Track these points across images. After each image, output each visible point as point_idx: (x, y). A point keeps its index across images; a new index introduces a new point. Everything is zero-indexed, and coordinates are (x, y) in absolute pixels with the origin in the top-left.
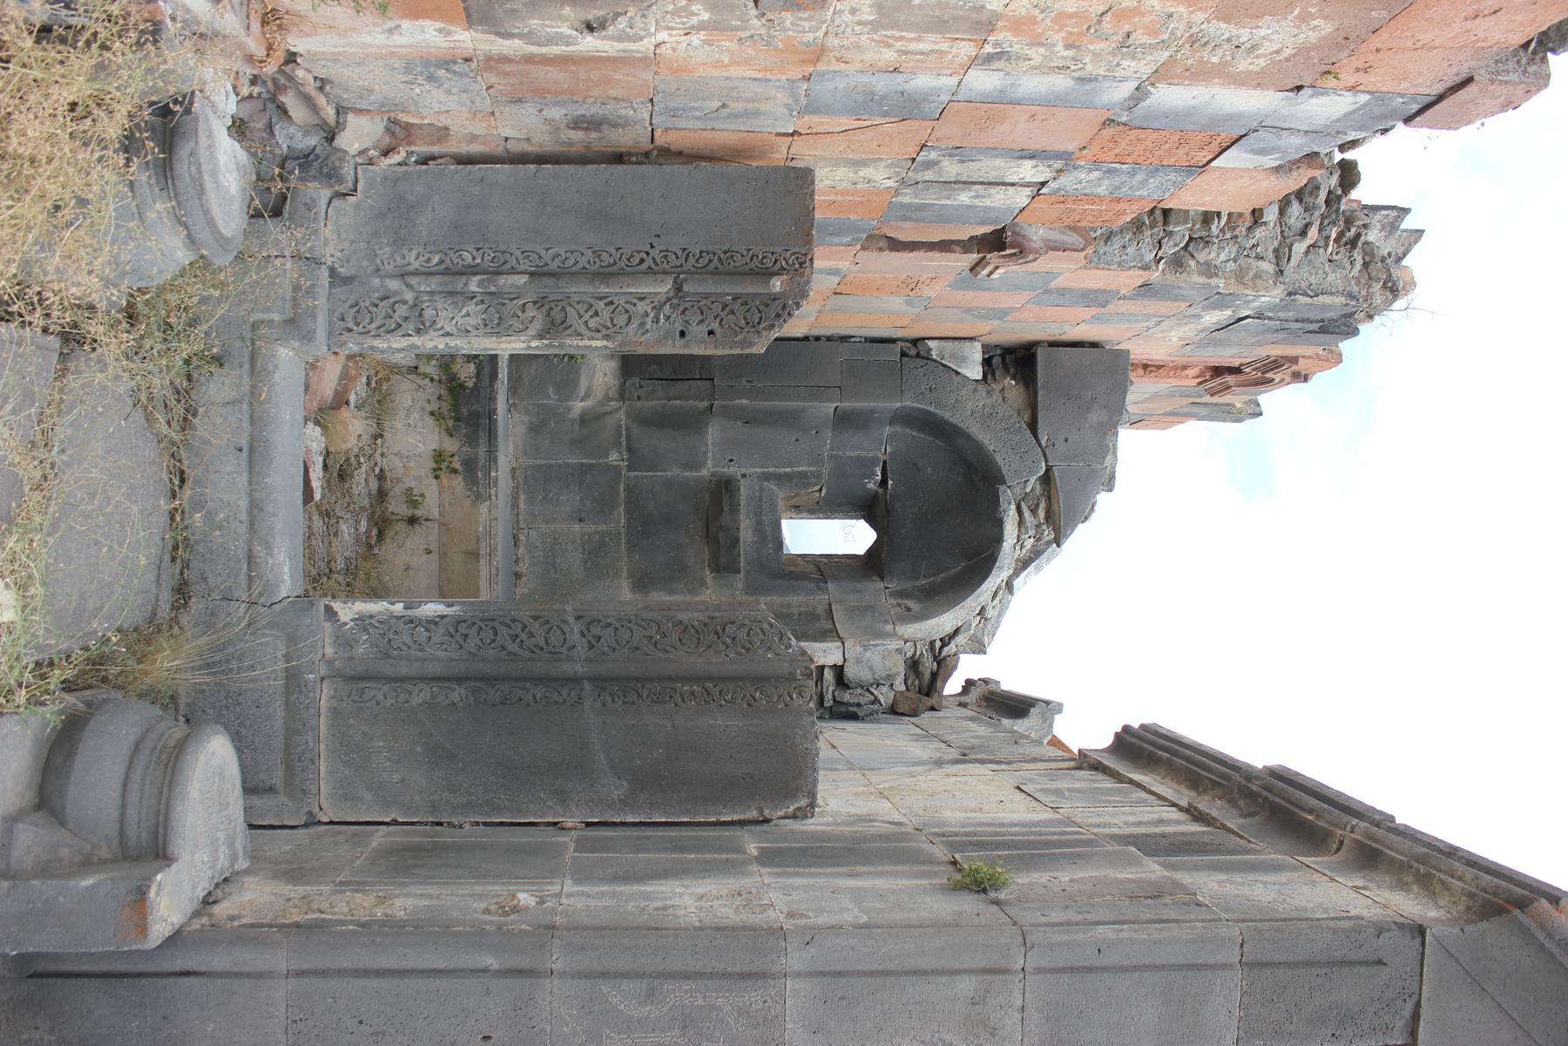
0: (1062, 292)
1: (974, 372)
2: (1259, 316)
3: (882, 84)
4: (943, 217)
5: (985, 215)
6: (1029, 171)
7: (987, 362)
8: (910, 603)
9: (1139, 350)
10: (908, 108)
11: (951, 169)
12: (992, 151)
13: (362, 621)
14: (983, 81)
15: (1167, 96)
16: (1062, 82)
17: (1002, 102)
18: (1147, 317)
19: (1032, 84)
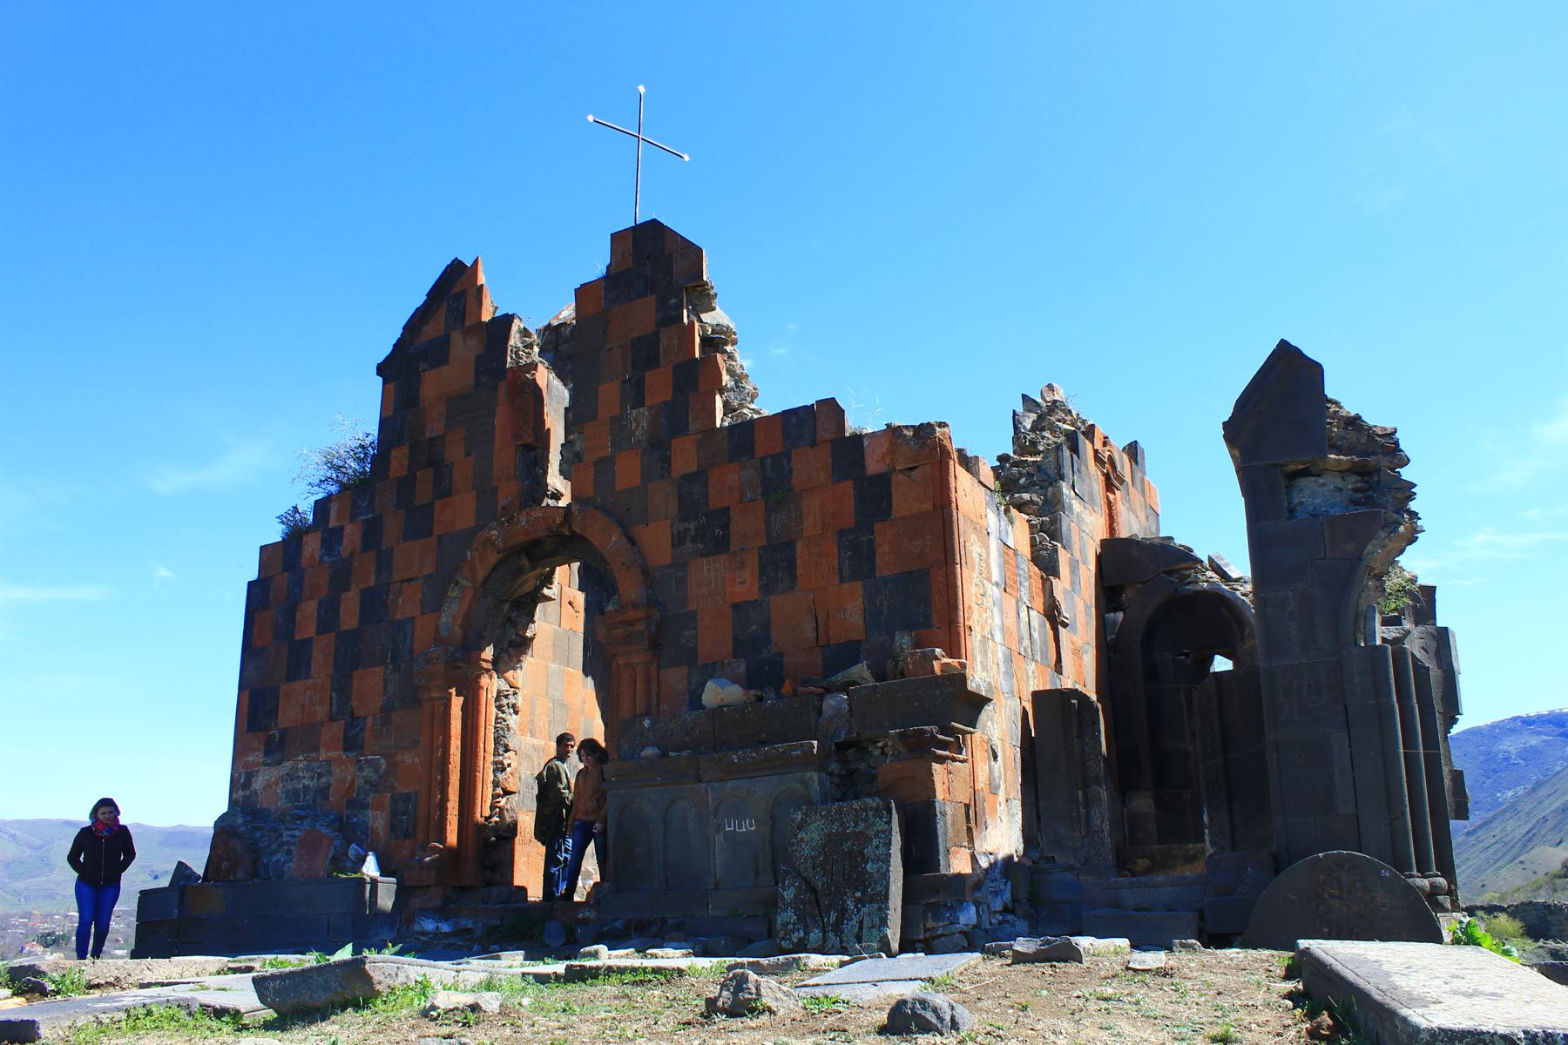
0: (1073, 583)
1: (1120, 616)
2: (1073, 487)
3: (1002, 669)
4: (1044, 643)
5: (1042, 626)
6: (1024, 614)
7: (1115, 610)
8: (1247, 632)
9: (1101, 533)
10: (1009, 660)
11: (1026, 642)
12: (1019, 629)
13: (1213, 844)
14: (998, 637)
15: (996, 576)
16: (996, 610)
17: (1003, 629)
18: (1081, 538)
19: (997, 621)
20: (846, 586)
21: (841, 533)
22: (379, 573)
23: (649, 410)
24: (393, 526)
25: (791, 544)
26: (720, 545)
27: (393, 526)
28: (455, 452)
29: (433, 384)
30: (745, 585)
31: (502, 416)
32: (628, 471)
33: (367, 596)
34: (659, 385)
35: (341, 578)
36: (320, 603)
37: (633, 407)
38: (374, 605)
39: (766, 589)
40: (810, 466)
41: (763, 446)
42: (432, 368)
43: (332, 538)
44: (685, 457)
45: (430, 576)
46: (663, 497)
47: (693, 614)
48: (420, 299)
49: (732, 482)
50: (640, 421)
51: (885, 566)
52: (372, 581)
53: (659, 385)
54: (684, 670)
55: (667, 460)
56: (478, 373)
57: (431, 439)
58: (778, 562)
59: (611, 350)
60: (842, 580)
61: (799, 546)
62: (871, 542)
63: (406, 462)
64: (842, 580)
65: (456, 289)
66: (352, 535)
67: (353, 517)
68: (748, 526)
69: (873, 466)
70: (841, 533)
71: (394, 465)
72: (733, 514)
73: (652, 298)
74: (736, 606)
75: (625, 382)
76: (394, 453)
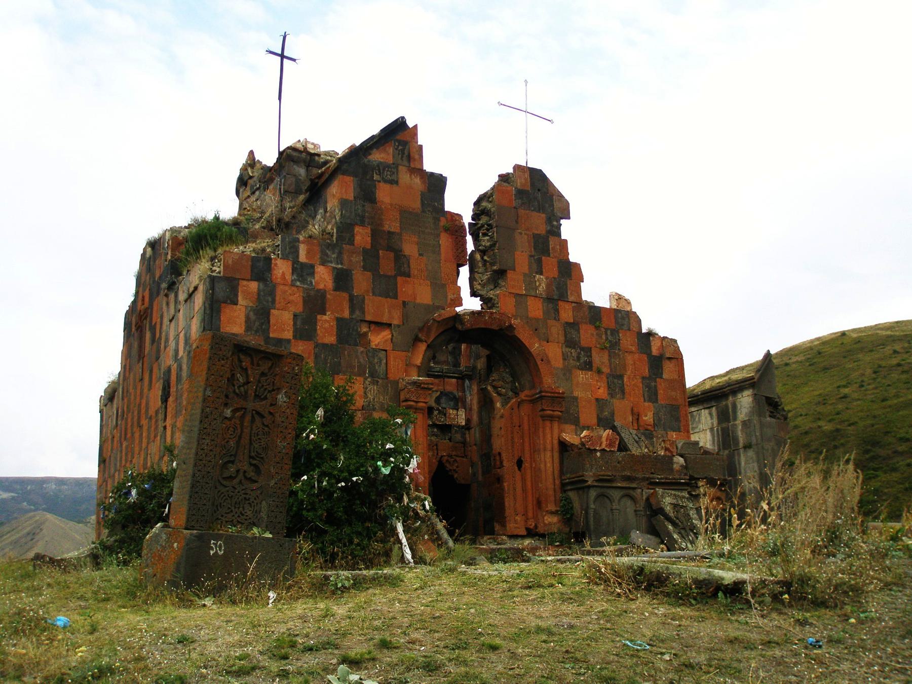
20: (646, 404)
21: (643, 378)
22: (352, 312)
23: (547, 278)
24: (361, 282)
25: (621, 377)
26: (588, 366)
27: (361, 282)
28: (410, 248)
29: (384, 194)
30: (602, 392)
31: (445, 241)
32: (536, 309)
33: (340, 321)
34: (551, 265)
35: (315, 303)
36: (295, 316)
37: (537, 273)
38: (348, 333)
39: (612, 396)
40: (627, 341)
41: (606, 322)
42: (386, 181)
43: (303, 271)
44: (567, 313)
45: (399, 326)
46: (556, 330)
47: (576, 399)
48: (375, 130)
49: (587, 335)
50: (542, 283)
51: (661, 401)
52: (346, 314)
53: (551, 265)
54: (573, 427)
55: (557, 311)
56: (423, 204)
57: (389, 232)
58: (615, 383)
59: (521, 233)
60: (645, 401)
61: (625, 379)
62: (656, 386)
63: (369, 239)
64: (645, 401)
65: (400, 136)
66: (323, 277)
67: (323, 263)
68: (600, 359)
69: (655, 351)
70: (643, 378)
71: (358, 239)
72: (594, 354)
73: (543, 215)
74: (597, 400)
75: (531, 256)
76: (357, 229)
